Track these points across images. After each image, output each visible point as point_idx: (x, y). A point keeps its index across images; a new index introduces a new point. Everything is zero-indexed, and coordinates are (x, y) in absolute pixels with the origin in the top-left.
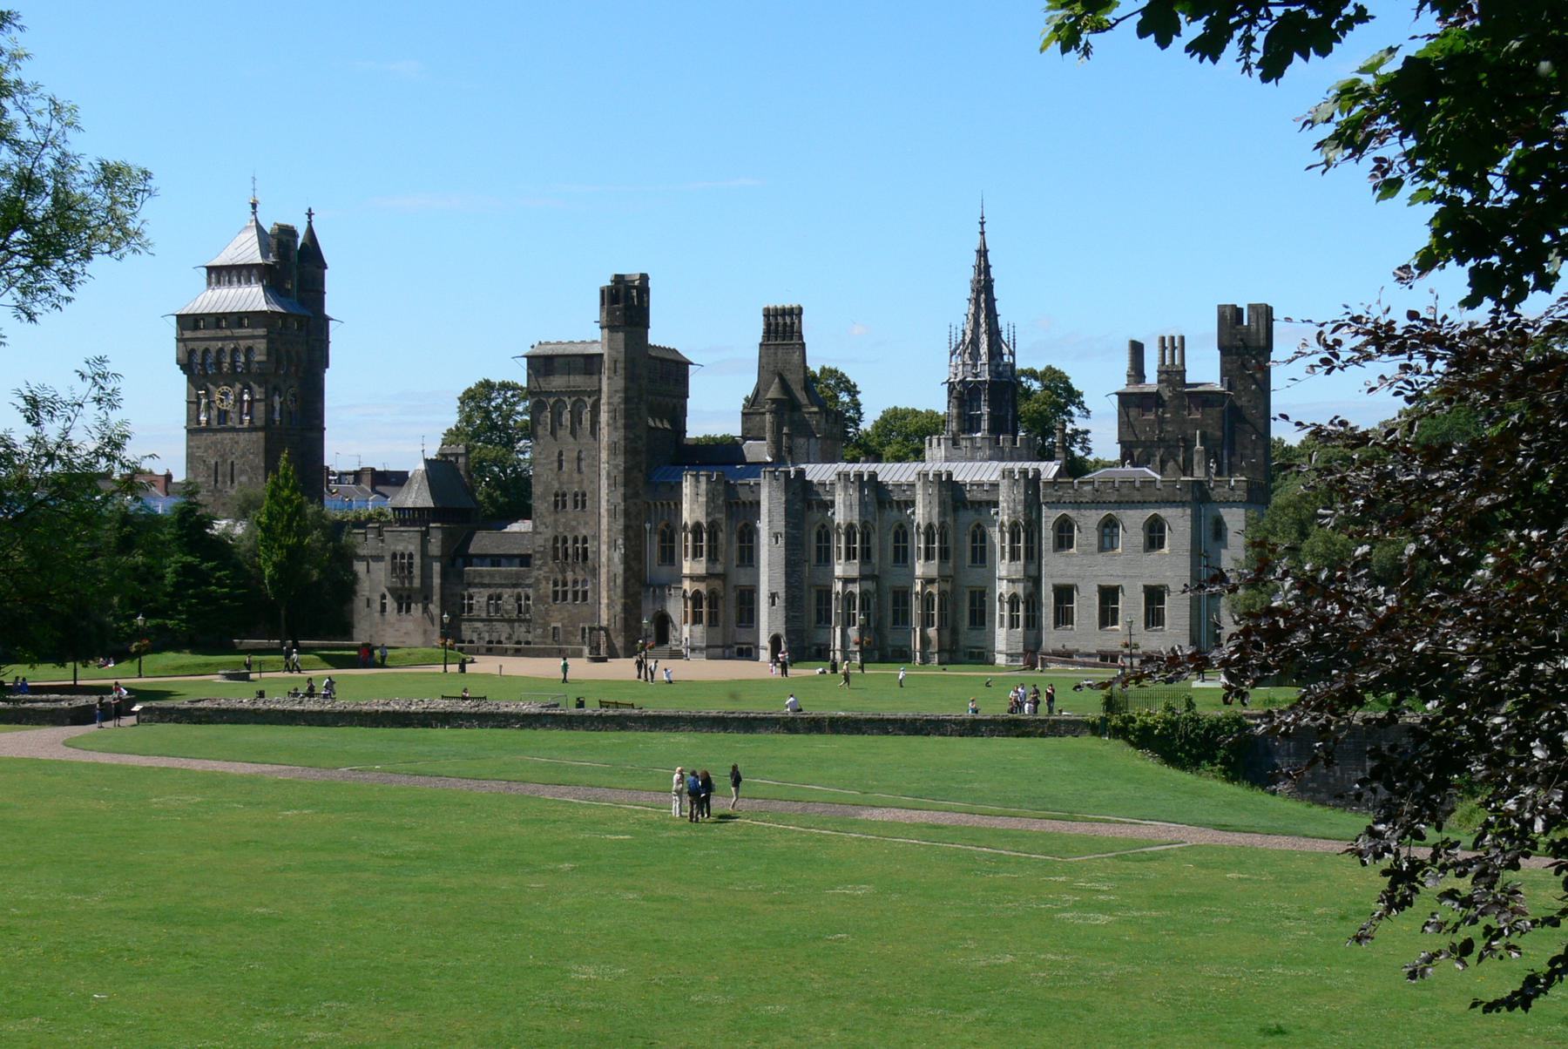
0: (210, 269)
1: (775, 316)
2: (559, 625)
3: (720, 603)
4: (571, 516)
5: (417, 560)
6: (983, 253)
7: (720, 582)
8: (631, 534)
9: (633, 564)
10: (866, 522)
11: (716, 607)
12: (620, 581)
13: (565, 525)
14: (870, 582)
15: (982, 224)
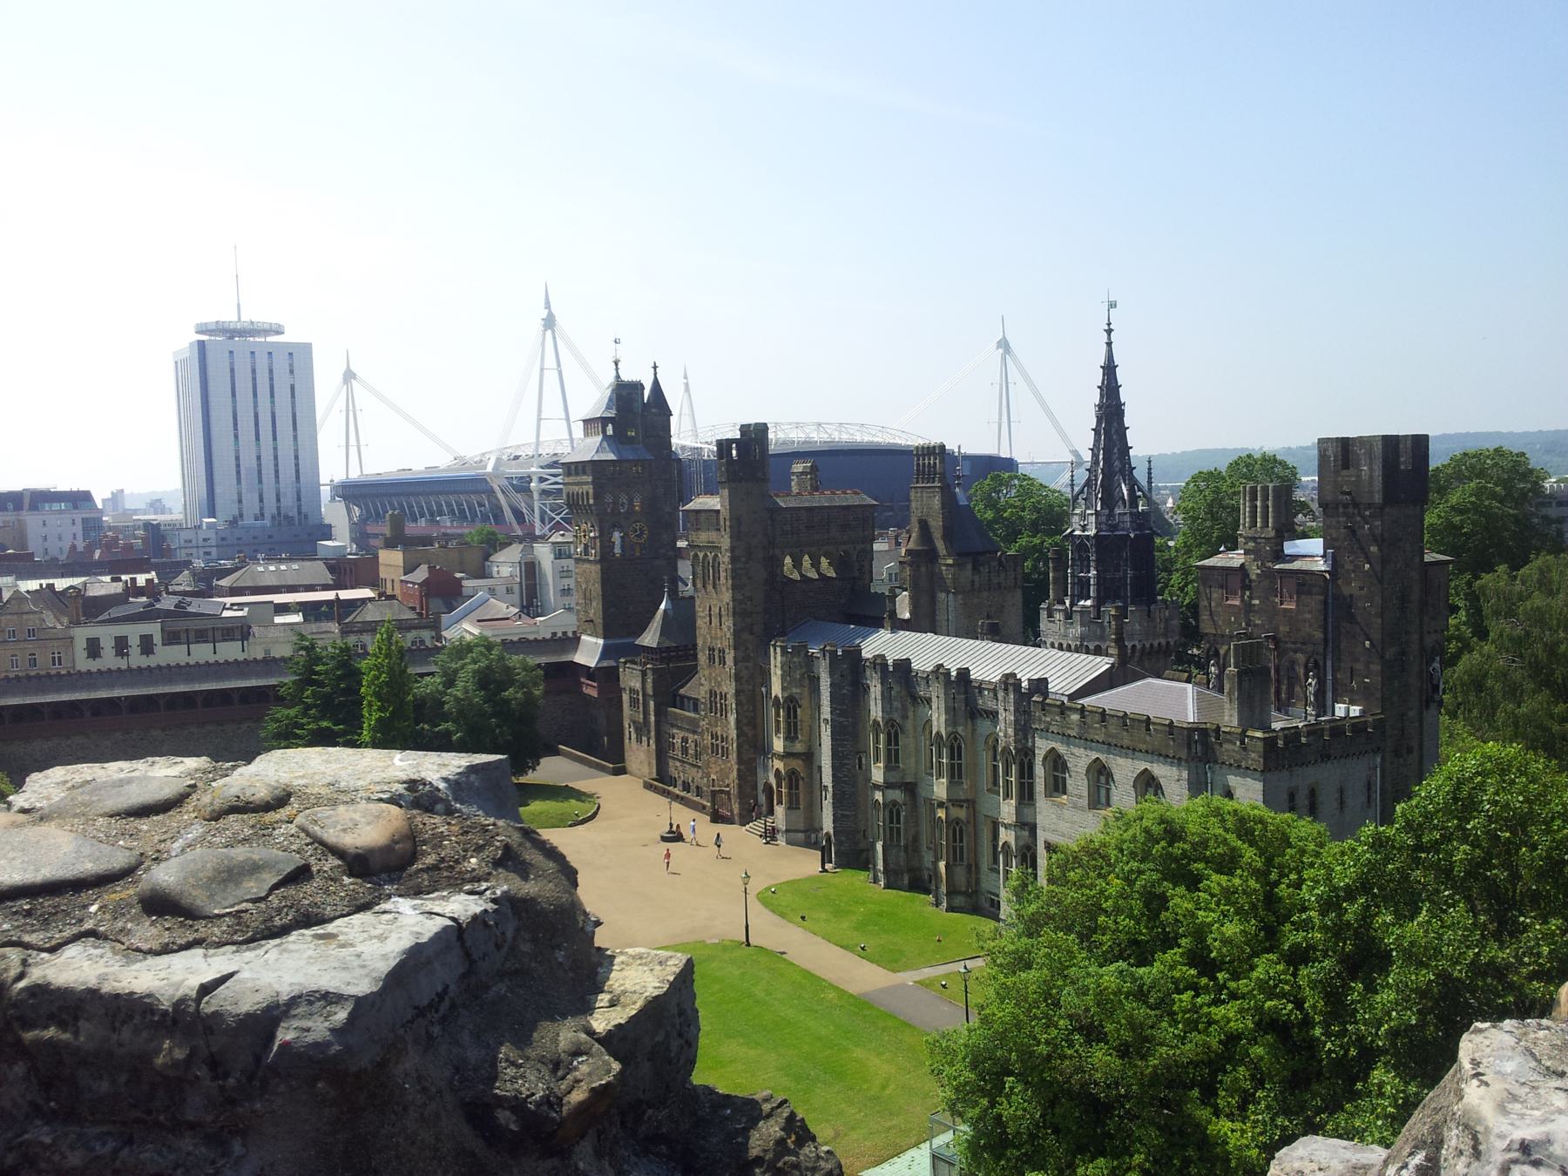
0: (584, 421)
1: (924, 455)
2: (715, 778)
3: (801, 783)
4: (717, 671)
5: (641, 698)
6: (1110, 369)
7: (800, 762)
8: (742, 697)
9: (745, 728)
10: (891, 720)
11: (797, 788)
12: (735, 745)
13: (716, 680)
14: (898, 792)
15: (1109, 332)
